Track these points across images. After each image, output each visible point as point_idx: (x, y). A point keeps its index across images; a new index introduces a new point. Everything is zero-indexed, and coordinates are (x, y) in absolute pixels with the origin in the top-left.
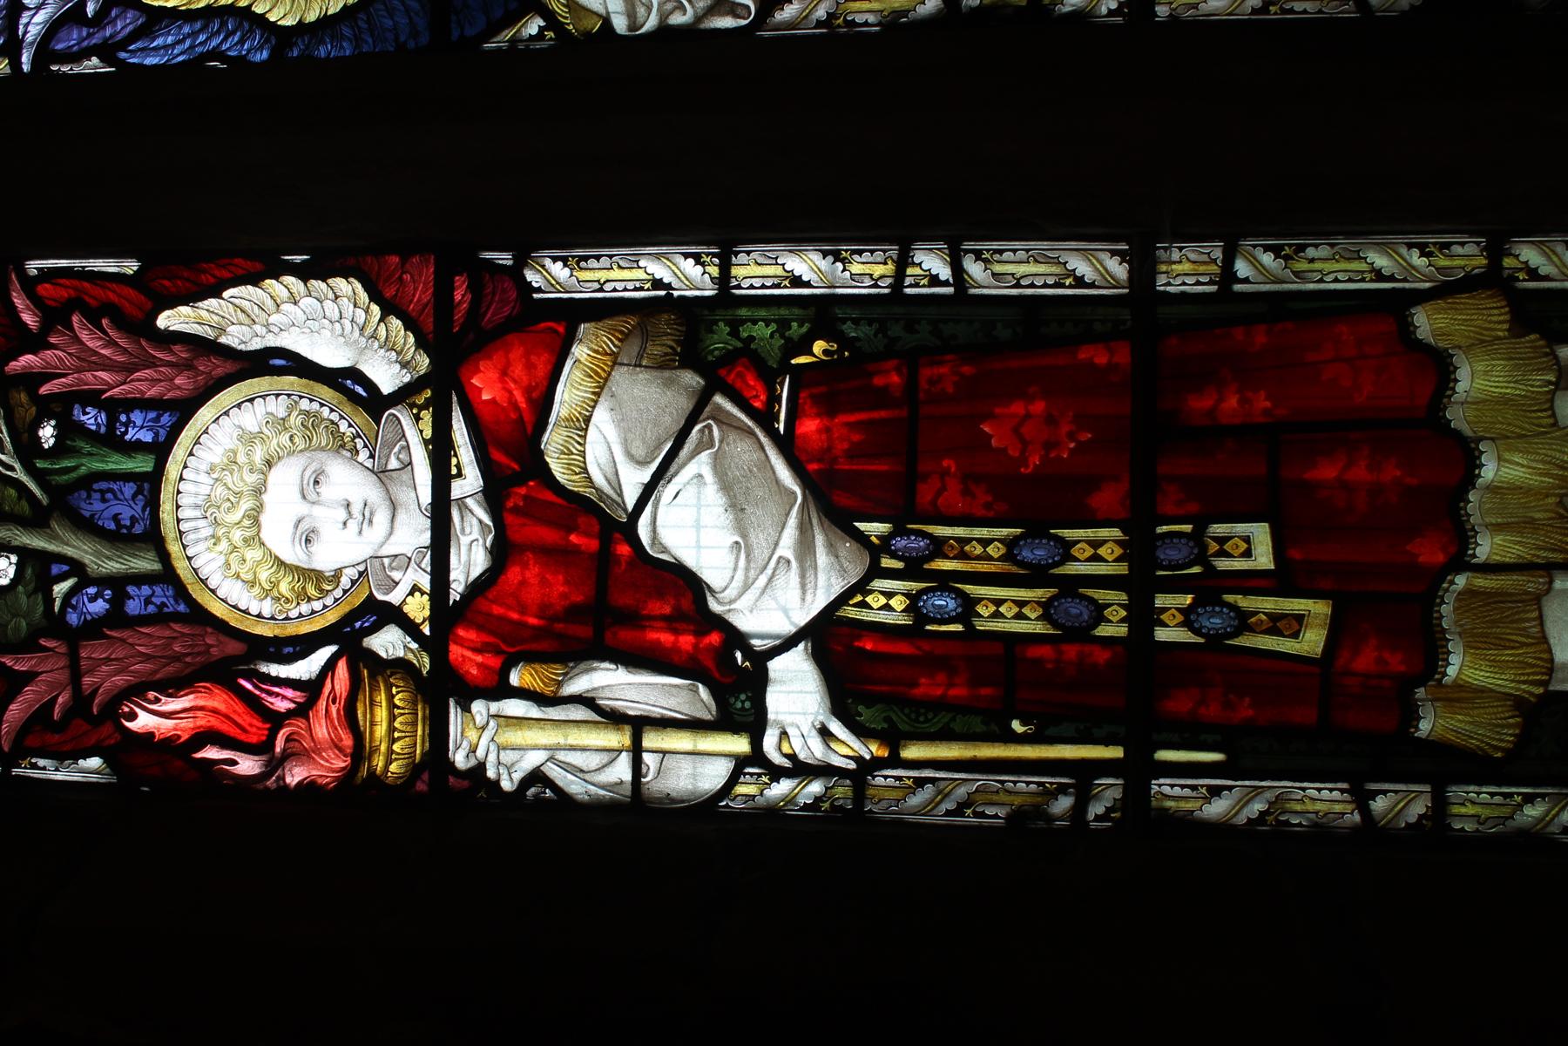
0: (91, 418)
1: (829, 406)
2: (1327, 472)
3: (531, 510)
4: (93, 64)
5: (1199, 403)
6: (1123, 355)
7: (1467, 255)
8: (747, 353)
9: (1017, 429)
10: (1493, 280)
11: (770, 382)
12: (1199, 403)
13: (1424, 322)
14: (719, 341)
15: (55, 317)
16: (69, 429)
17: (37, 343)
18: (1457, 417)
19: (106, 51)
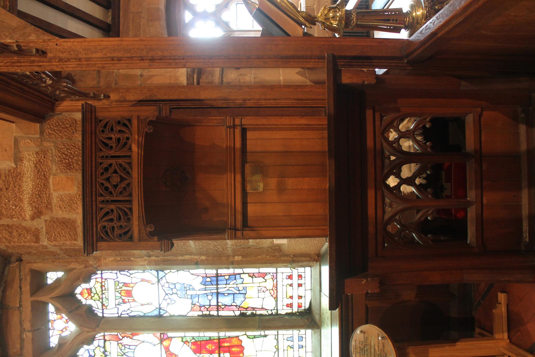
0: (128, 347)
1: (194, 345)
2: (233, 349)
3: (169, 354)
4: (127, 315)
5: (223, 344)
6: (217, 341)
7: (244, 333)
8: (187, 341)
9: (209, 347)
10: (246, 334)
11: (189, 343)
12: (223, 344)
13: (240, 338)
14: (184, 340)
15: (123, 337)
16: (125, 347)
17: (121, 340)
18: (242, 345)
19: (128, 314)
